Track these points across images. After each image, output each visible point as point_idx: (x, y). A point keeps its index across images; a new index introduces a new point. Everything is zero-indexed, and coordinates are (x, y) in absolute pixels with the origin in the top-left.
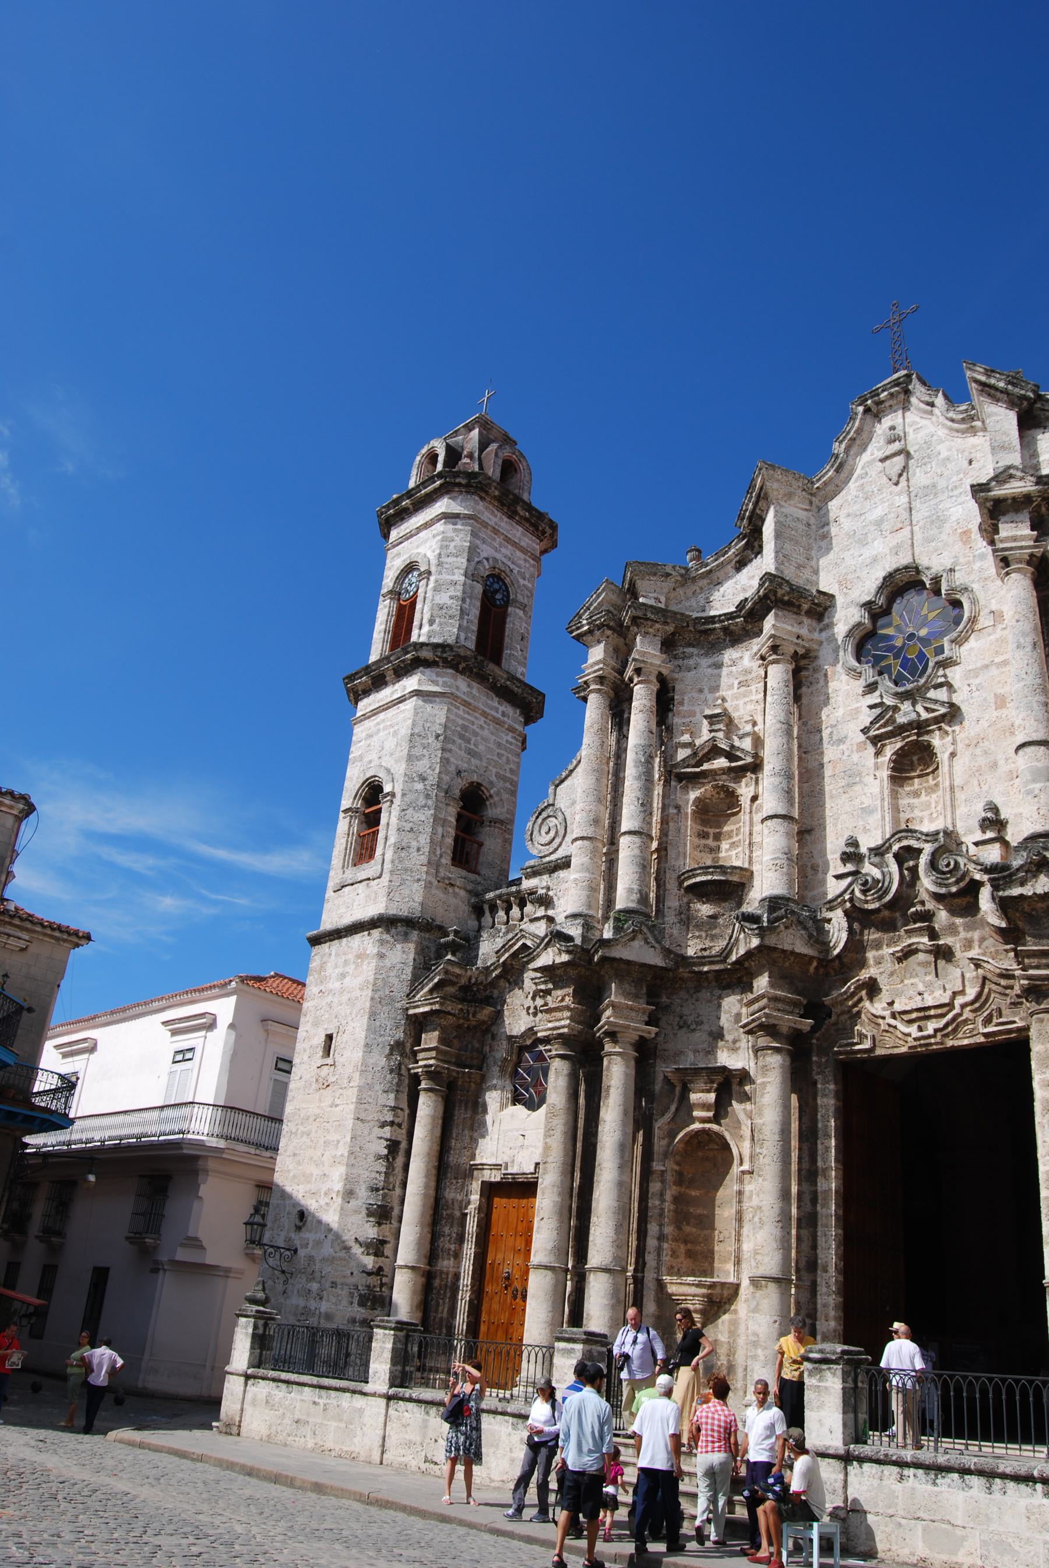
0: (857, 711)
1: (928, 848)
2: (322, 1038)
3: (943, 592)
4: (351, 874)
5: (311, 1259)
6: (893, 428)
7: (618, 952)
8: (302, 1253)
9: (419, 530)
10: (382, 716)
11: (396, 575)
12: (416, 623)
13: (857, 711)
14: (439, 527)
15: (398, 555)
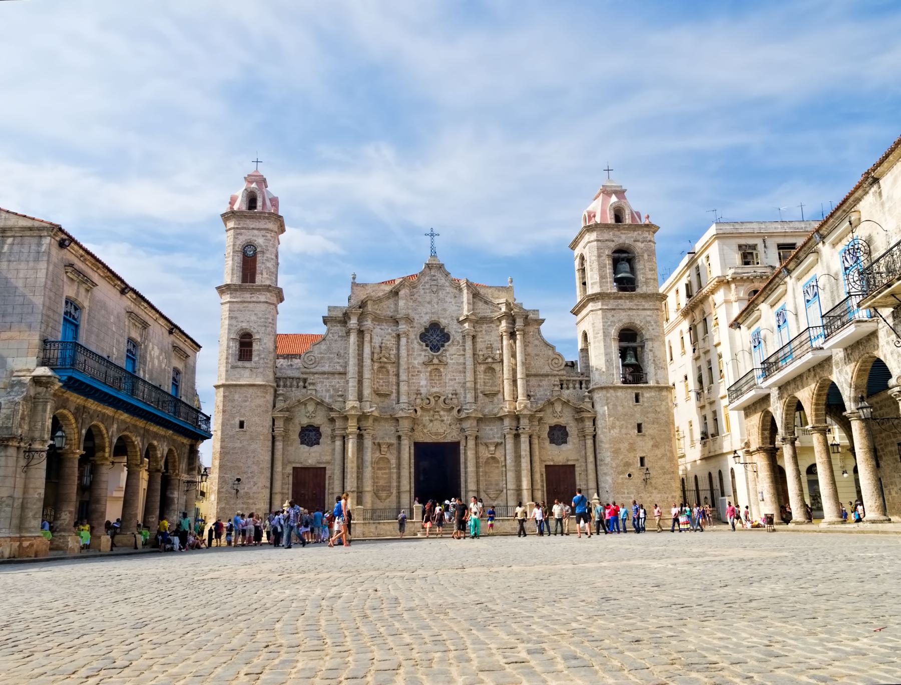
0: (421, 355)
1: (442, 398)
2: (238, 423)
3: (446, 331)
4: (240, 363)
5: (247, 493)
6: (434, 276)
7: (374, 414)
8: (241, 491)
9: (253, 229)
10: (246, 305)
11: (242, 244)
12: (258, 271)
13: (421, 355)
14: (263, 232)
15: (241, 234)
